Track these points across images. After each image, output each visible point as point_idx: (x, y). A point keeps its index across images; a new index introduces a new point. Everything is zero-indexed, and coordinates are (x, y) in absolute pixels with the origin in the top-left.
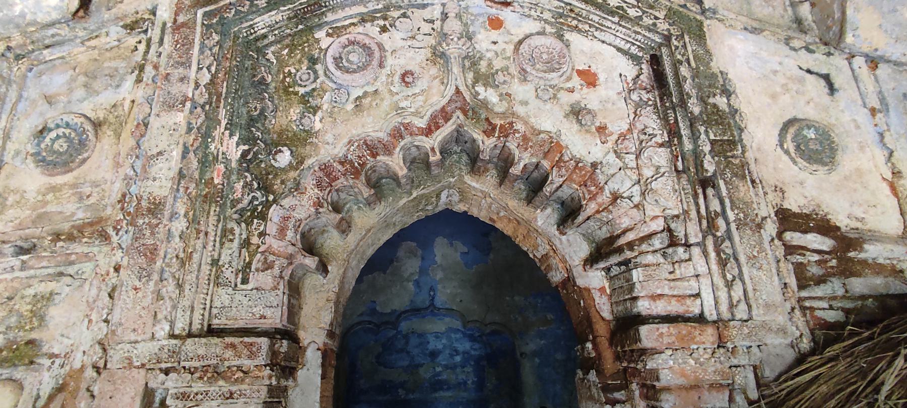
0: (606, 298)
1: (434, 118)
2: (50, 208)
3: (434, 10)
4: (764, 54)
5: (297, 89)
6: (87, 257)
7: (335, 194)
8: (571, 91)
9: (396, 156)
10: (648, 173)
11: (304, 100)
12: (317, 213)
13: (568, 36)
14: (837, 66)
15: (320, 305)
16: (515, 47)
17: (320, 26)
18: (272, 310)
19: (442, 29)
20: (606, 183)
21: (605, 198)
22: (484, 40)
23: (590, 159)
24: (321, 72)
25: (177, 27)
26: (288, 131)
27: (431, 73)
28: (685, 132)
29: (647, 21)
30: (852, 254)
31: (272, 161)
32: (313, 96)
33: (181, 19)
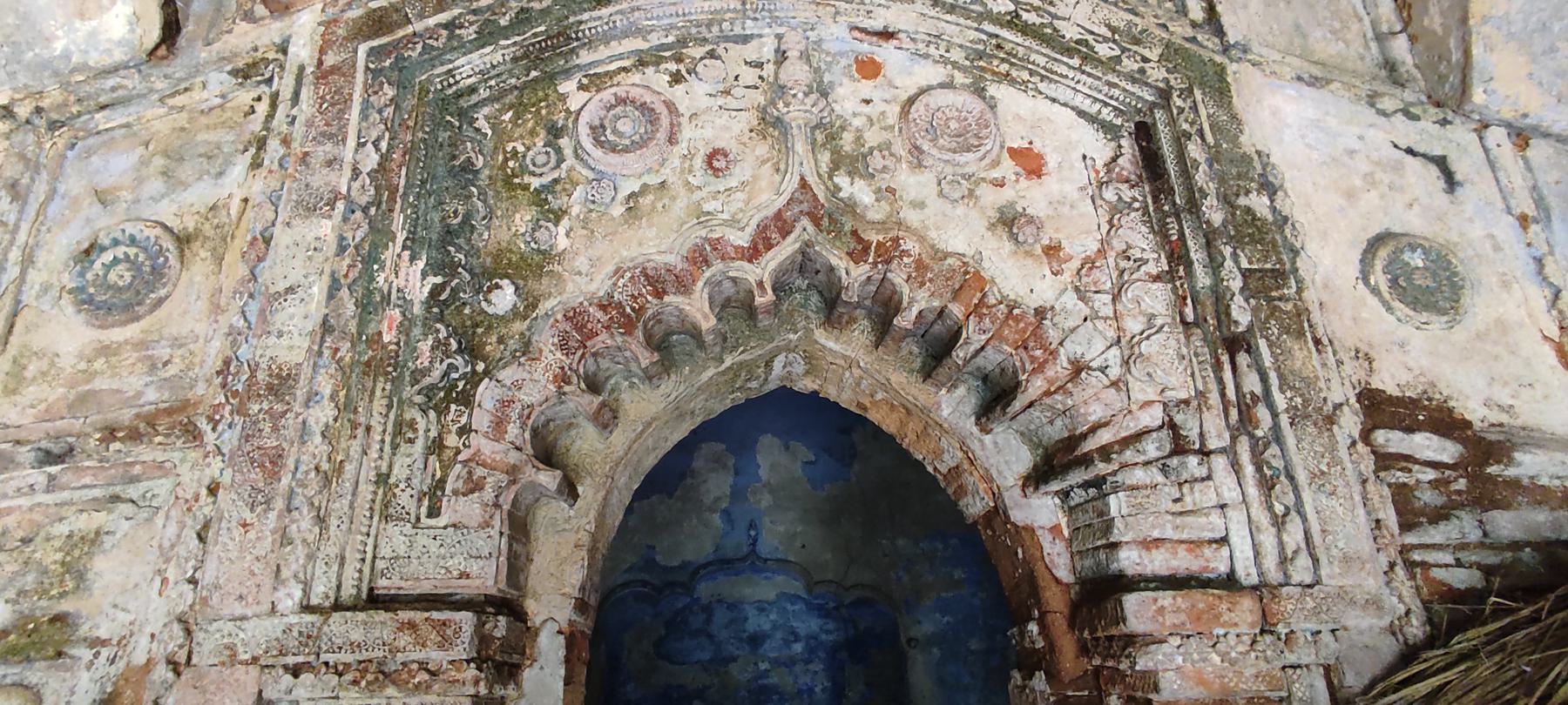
1: (762, 229)
2: (100, 384)
3: (763, 45)
4: (1332, 122)
5: (527, 179)
6: (161, 469)
7: (591, 361)
8: (1000, 184)
9: (696, 295)
10: (1134, 326)
11: (539, 198)
14: (1458, 141)
15: (563, 554)
17: (567, 73)
18: (481, 563)
20: (1061, 344)
21: (1059, 369)
22: (849, 96)
23: (1033, 302)
24: (568, 152)
25: (322, 74)
26: (511, 251)
28: (1197, 255)
29: (1130, 65)
30: (1493, 469)
33: (330, 60)
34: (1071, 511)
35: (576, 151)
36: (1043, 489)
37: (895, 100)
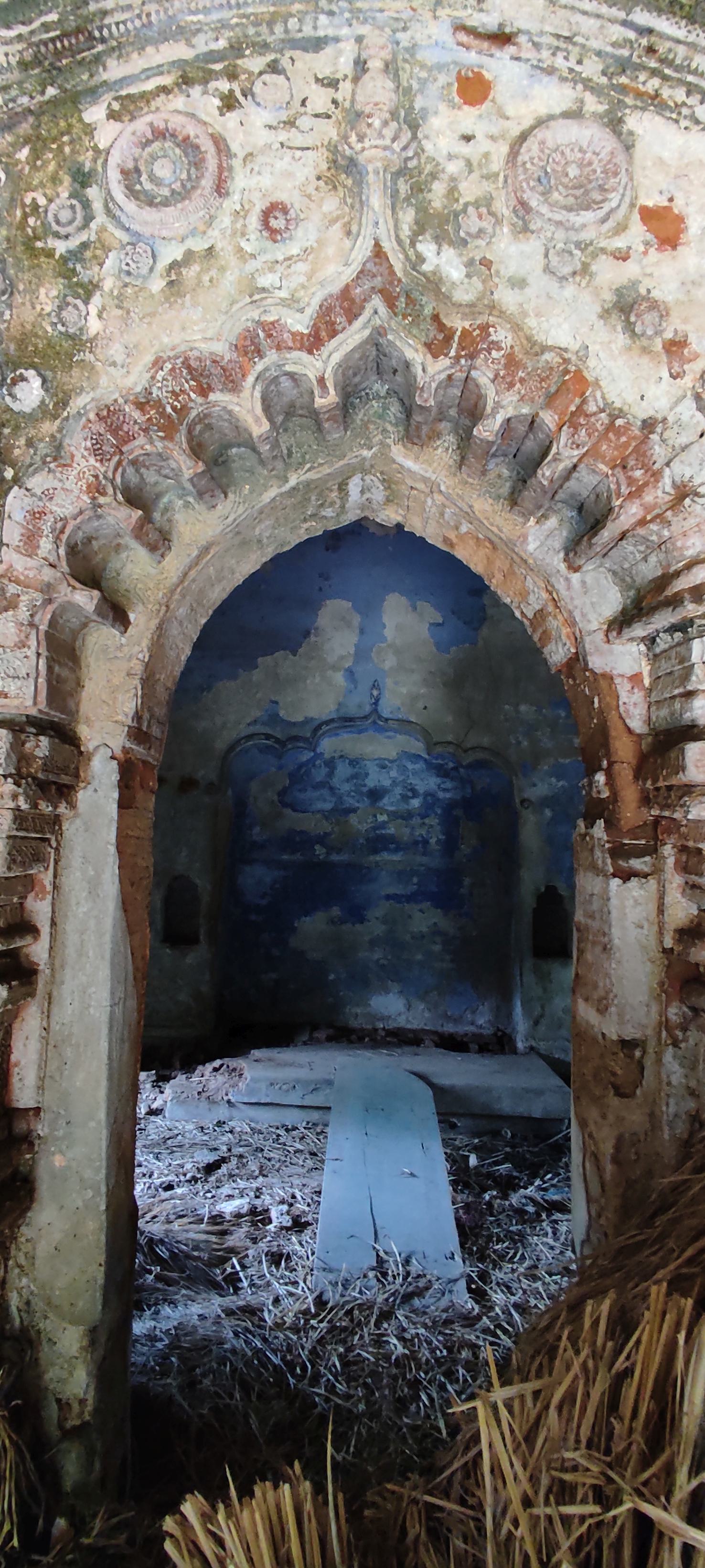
0: (642, 694)
1: (325, 312)
3: (340, 53)
5: (52, 243)
7: (130, 471)
8: (623, 256)
9: (246, 393)
11: (66, 268)
12: (96, 506)
13: (634, 122)
15: (116, 681)
16: (512, 147)
17: (93, 93)
19: (353, 101)
20: (668, 464)
21: (660, 494)
22: (446, 129)
23: (642, 412)
24: (98, 206)
26: (36, 336)
27: (326, 208)
31: (8, 399)
32: (82, 260)
34: (655, 658)
35: (106, 206)
36: (628, 633)
37: (503, 137)
